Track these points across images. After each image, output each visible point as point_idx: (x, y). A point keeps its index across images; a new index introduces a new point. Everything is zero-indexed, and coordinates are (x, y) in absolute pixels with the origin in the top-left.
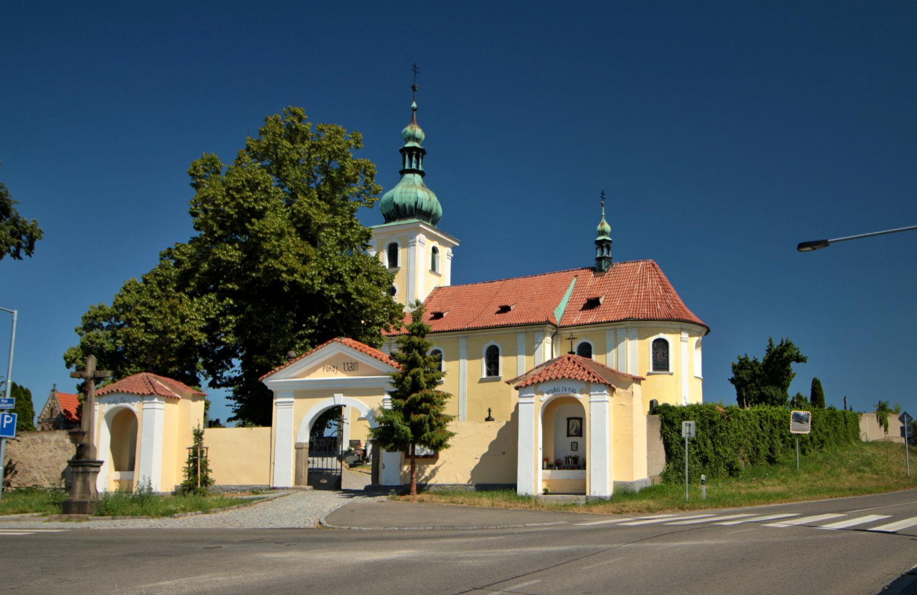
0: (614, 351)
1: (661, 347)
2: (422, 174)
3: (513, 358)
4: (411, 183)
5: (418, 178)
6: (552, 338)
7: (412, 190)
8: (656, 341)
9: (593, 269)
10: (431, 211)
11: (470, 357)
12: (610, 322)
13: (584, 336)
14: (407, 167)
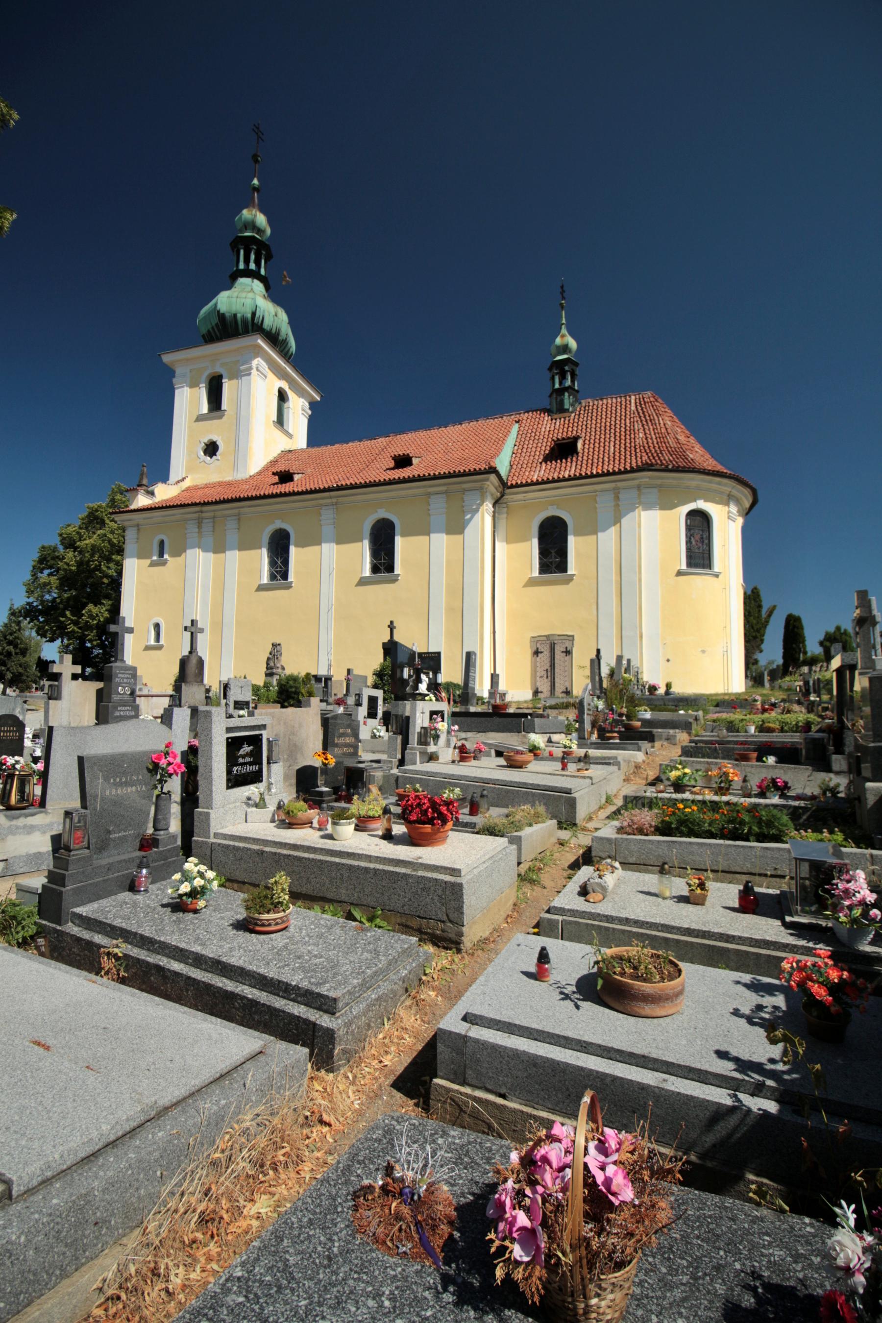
0: (613, 530)
2: (263, 280)
3: (424, 539)
4: (249, 289)
5: (258, 286)
6: (494, 505)
7: (247, 297)
9: (549, 411)
10: (278, 333)
11: (341, 539)
12: (608, 474)
14: (242, 266)
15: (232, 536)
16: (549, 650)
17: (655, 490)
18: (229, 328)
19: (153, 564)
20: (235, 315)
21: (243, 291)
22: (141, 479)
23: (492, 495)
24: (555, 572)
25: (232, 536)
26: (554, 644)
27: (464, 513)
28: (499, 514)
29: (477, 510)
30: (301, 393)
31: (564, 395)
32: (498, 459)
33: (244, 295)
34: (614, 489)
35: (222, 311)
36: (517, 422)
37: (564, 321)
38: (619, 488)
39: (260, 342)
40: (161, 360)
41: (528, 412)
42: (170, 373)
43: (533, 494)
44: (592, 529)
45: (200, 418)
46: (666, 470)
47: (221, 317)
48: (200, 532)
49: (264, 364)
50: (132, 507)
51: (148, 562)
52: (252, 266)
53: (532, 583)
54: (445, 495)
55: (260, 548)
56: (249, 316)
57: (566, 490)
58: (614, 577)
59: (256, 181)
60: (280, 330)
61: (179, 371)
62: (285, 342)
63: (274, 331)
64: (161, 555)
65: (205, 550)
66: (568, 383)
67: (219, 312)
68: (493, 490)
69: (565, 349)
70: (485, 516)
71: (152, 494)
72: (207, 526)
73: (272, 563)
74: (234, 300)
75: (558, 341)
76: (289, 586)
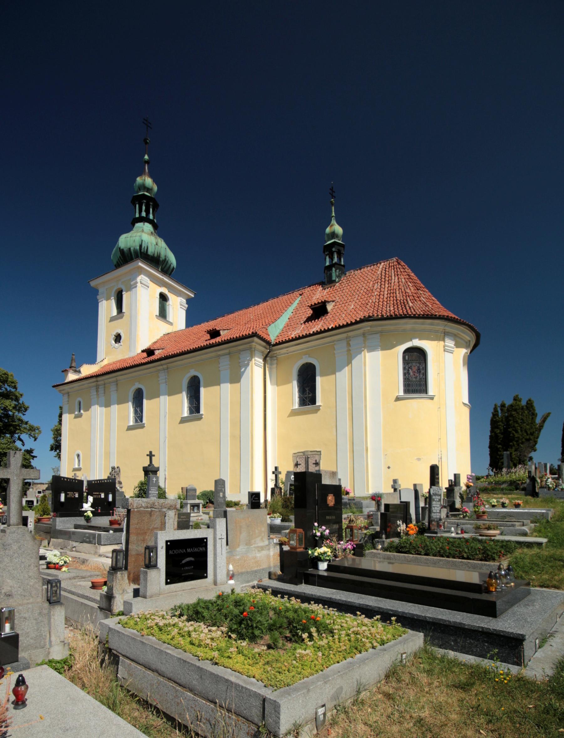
0: (347, 369)
1: (416, 360)
2: (151, 222)
3: (216, 388)
5: (148, 227)
6: (265, 360)
8: (408, 351)
9: (322, 284)
10: (159, 256)
11: (171, 393)
12: (340, 327)
13: (306, 354)
14: (137, 215)
15: (114, 396)
16: (304, 463)
17: (378, 335)
18: (126, 257)
19: (76, 417)
20: (130, 249)
21: (137, 232)
22: (71, 363)
23: (263, 352)
24: (309, 405)
25: (114, 396)
26: (308, 458)
27: (240, 367)
28: (271, 364)
29: (248, 365)
30: (178, 293)
31: (332, 270)
32: (273, 325)
33: (134, 235)
34: (347, 338)
35: (122, 248)
36: (300, 295)
37: (333, 214)
38: (350, 337)
39: (140, 264)
40: (90, 285)
41: (310, 286)
42: (95, 292)
43: (293, 348)
44: (332, 370)
45: (112, 319)
46: (383, 319)
47: (122, 251)
48: (98, 394)
49: (147, 278)
50: (66, 381)
51: (73, 415)
52: (144, 214)
53: (294, 413)
54: (228, 356)
55: (128, 402)
56: (138, 248)
57: (314, 343)
58: (348, 405)
59: (146, 157)
60: (160, 254)
61: (101, 291)
62: (165, 261)
63: (156, 255)
64: (80, 411)
65: (100, 406)
66: (336, 260)
67: (120, 248)
68: (263, 349)
69: (333, 235)
70: (256, 369)
71: (79, 372)
72: (101, 390)
73: (136, 412)
74: (129, 239)
75: (328, 230)
76: (143, 427)
